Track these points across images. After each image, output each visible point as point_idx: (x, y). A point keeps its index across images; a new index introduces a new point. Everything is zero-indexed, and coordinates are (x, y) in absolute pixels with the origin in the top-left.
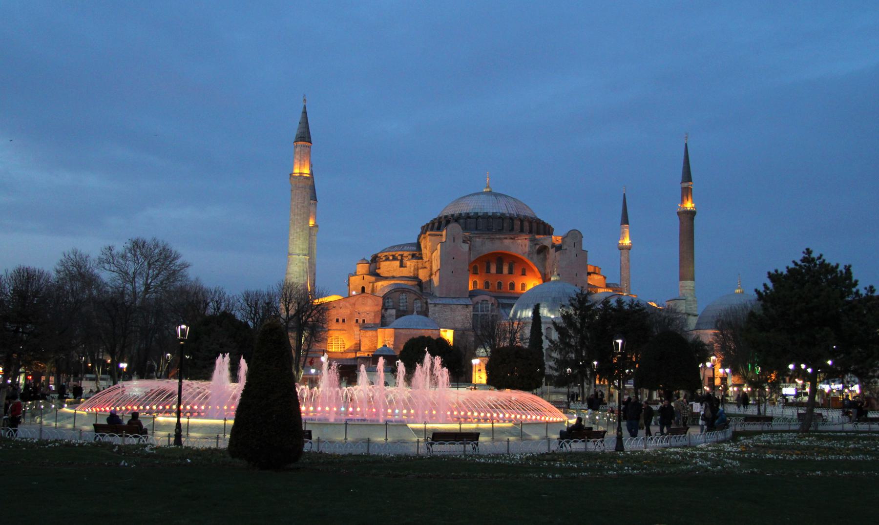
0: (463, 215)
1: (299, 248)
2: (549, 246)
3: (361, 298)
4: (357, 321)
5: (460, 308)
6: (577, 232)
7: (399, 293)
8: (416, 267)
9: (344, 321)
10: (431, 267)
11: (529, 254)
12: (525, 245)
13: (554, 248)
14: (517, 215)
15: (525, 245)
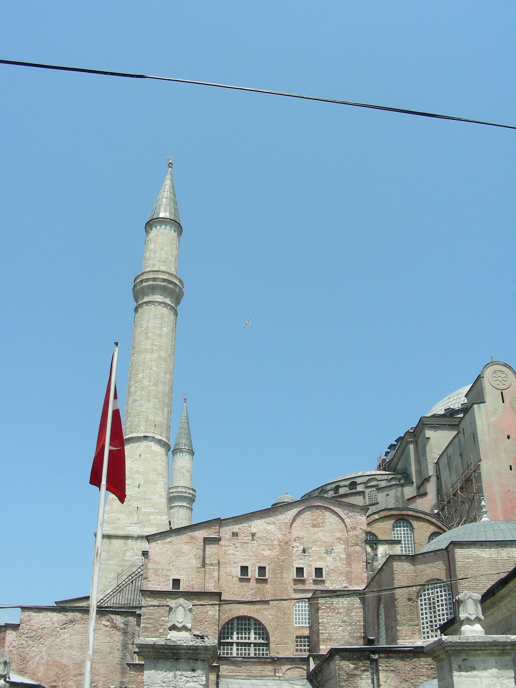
9: (262, 569)
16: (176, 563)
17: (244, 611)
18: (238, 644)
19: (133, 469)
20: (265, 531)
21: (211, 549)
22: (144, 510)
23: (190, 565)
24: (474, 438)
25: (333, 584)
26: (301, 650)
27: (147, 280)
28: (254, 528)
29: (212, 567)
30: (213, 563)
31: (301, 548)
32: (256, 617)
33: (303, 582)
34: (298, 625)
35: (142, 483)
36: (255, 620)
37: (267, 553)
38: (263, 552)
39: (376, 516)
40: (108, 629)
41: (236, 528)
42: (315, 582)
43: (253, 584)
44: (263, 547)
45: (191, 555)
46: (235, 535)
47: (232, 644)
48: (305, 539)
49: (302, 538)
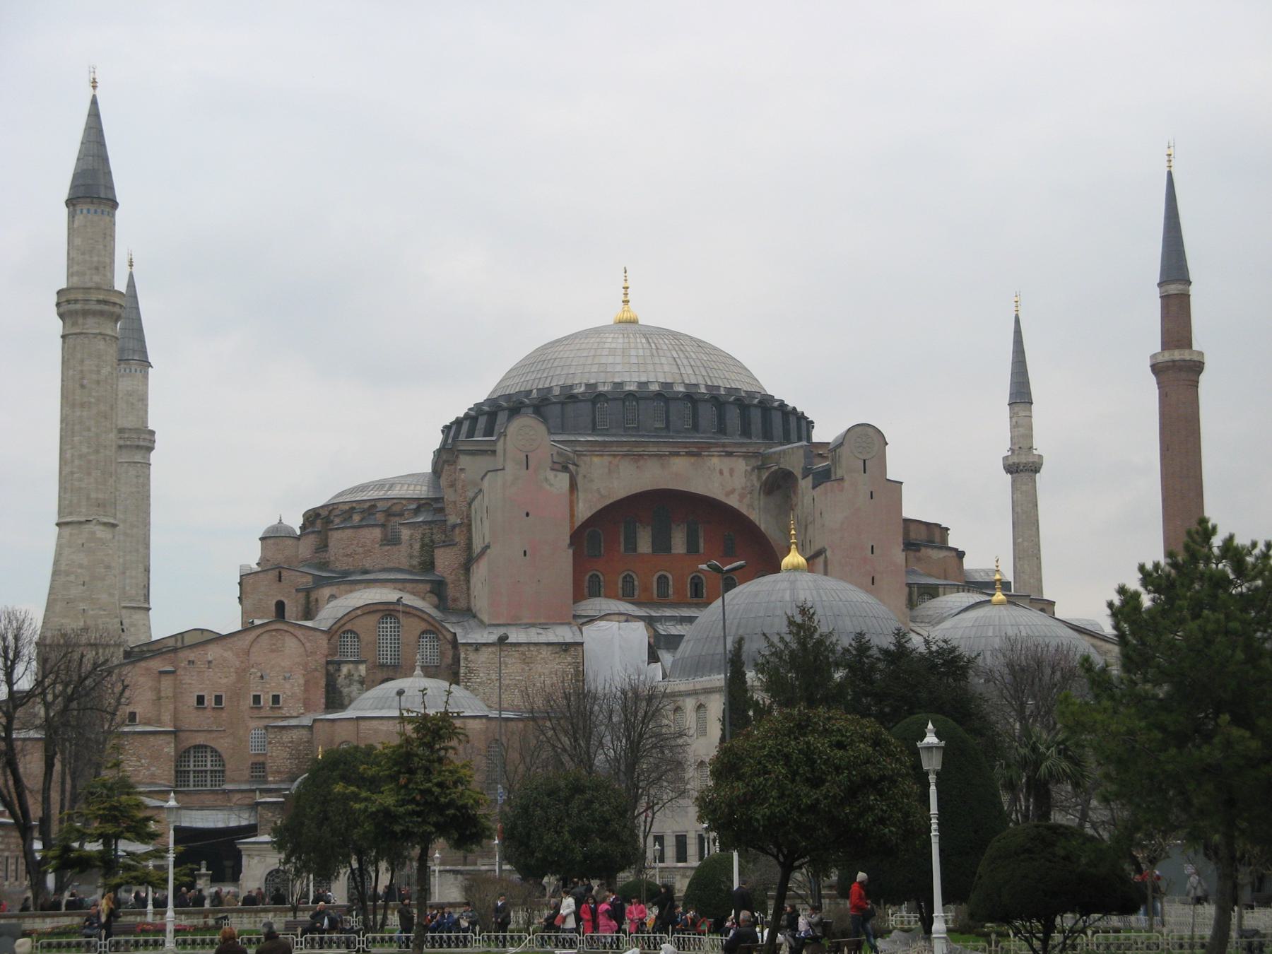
0: (557, 391)
1: (88, 498)
2: (798, 472)
3: (266, 636)
4: (257, 699)
5: (545, 653)
6: (870, 430)
7: (379, 615)
8: (427, 540)
9: (218, 699)
10: (470, 539)
11: (742, 497)
12: (732, 471)
13: (811, 476)
14: (707, 386)
15: (732, 471)
17: (200, 739)
18: (194, 772)
21: (166, 682)
26: (256, 776)
27: (76, 301)
31: (259, 674)
32: (212, 745)
34: (253, 752)
35: (87, 579)
36: (212, 748)
37: (224, 681)
38: (220, 680)
39: (359, 612)
41: (192, 655)
43: (209, 713)
44: (219, 674)
46: (191, 662)
47: (189, 772)
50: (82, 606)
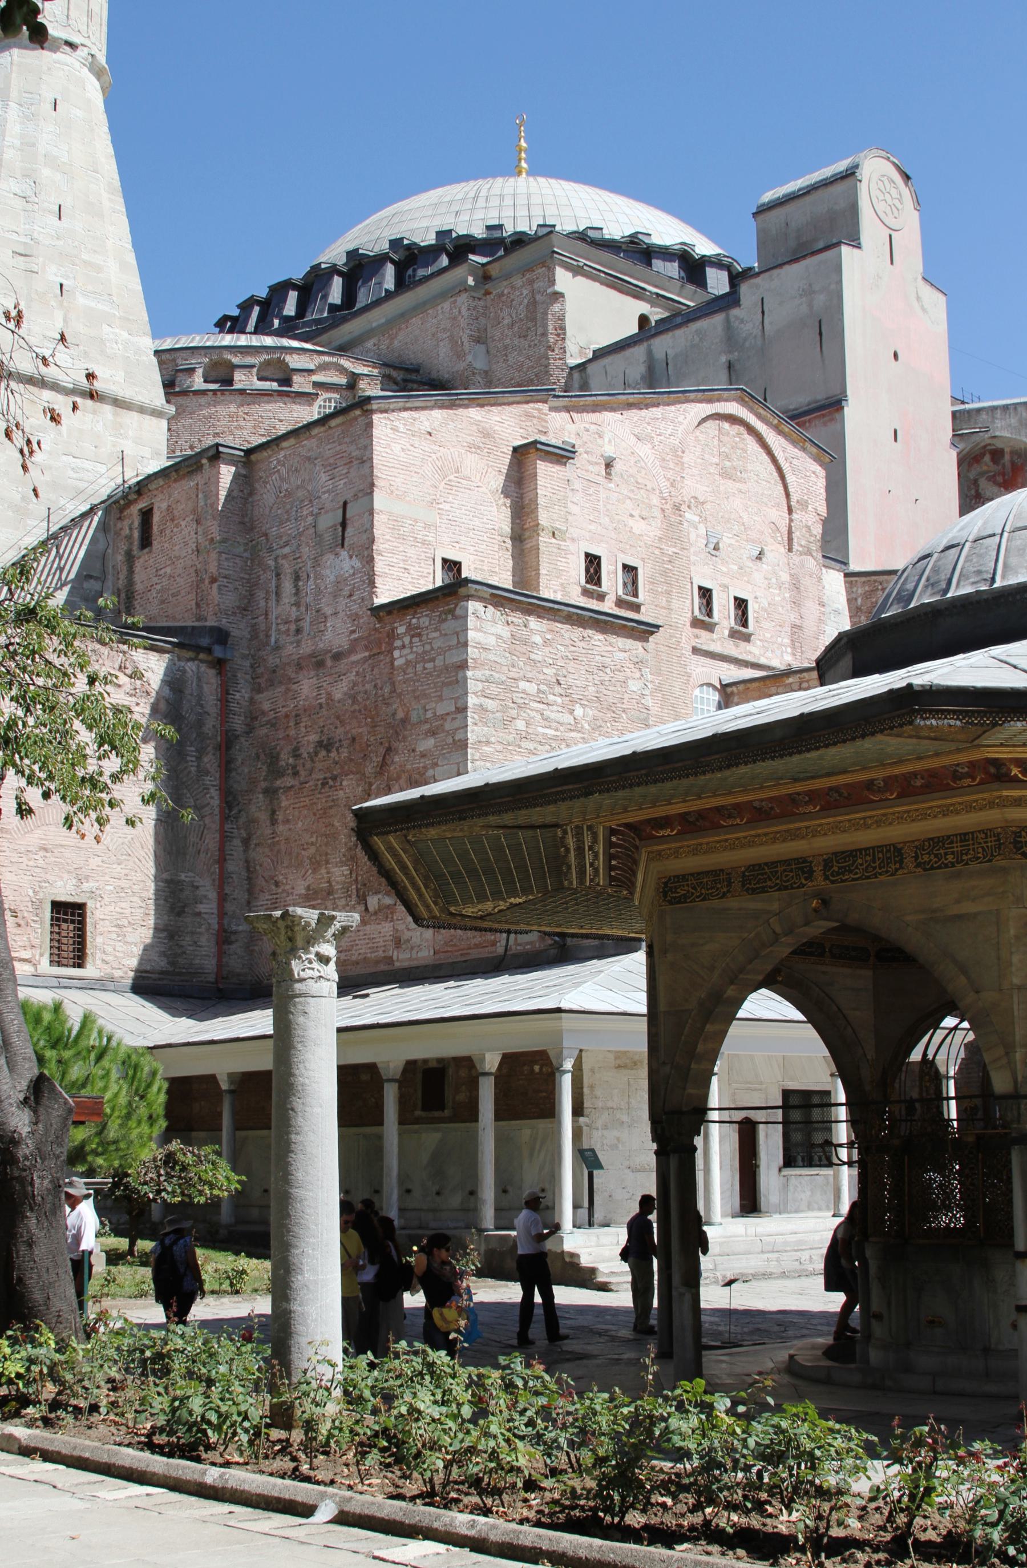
16: (447, 507)
19: (34, 145)
20: (632, 460)
22: (81, 300)
23: (485, 520)
24: (821, 334)
25: (766, 649)
28: (610, 441)
29: (553, 541)
30: (557, 529)
33: (710, 627)
38: (631, 522)
40: (122, 696)
42: (733, 634)
45: (483, 489)
48: (708, 506)
49: (703, 503)
50: (53, 275)
